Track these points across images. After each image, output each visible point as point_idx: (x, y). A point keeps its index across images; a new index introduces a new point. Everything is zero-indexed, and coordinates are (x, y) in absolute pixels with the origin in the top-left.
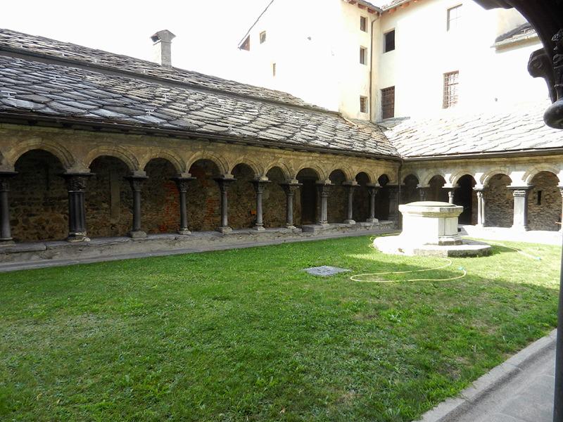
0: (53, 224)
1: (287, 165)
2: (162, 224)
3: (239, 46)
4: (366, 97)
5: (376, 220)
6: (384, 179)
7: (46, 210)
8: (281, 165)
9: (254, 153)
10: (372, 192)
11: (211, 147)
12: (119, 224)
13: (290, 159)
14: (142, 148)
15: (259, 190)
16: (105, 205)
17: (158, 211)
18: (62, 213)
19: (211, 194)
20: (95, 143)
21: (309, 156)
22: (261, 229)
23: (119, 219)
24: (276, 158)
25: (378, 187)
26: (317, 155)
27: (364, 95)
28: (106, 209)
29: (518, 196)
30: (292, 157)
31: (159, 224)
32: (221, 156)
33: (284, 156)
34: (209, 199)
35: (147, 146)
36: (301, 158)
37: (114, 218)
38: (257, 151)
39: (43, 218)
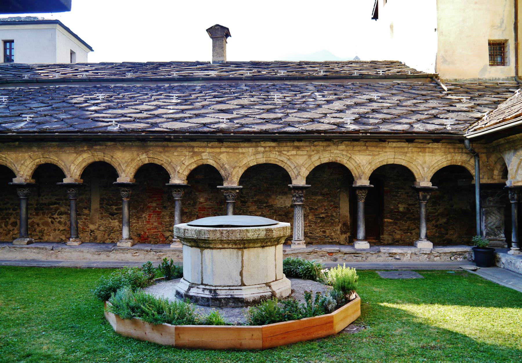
0: (42, 227)
1: (217, 161)
2: (142, 233)
3: (373, 16)
4: (506, 41)
7: (37, 214)
12: (98, 229)
14: (20, 154)
15: (174, 195)
16: (86, 211)
17: (139, 218)
18: (50, 218)
19: (202, 200)
21: (257, 146)
23: (97, 225)
27: (497, 36)
28: (87, 215)
30: (223, 150)
31: (139, 232)
32: (112, 157)
33: (208, 150)
34: (200, 206)
35: (26, 152)
37: (93, 224)
38: (164, 146)
39: (35, 221)
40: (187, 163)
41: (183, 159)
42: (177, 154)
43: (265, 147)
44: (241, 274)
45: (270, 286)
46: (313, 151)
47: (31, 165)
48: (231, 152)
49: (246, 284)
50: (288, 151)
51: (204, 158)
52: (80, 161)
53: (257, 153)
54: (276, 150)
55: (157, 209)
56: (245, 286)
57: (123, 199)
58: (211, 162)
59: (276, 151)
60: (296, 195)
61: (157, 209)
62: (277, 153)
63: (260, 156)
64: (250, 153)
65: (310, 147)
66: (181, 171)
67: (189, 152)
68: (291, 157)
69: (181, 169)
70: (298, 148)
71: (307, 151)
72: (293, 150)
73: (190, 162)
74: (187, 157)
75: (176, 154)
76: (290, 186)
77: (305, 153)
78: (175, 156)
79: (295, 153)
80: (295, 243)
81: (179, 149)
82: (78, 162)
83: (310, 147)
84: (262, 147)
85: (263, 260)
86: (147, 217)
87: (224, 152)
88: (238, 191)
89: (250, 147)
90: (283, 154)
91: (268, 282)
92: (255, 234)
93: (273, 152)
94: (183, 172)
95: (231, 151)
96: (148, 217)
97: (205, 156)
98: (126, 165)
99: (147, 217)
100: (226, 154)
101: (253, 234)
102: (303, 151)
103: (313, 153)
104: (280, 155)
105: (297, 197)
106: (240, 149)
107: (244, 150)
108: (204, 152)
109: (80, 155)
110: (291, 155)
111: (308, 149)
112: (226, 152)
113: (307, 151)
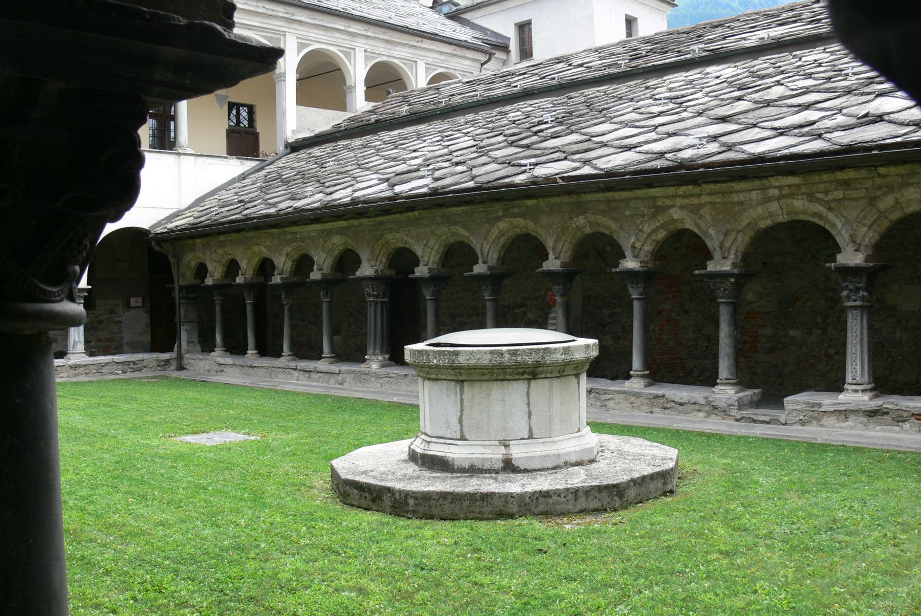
11: (516, 210)
13: (700, 206)
14: (422, 230)
15: (631, 290)
20: (379, 232)
21: (764, 188)
30: (705, 199)
33: (679, 202)
36: (735, 198)
40: (647, 229)
41: (639, 222)
42: (629, 214)
44: (460, 421)
45: (506, 446)
46: (879, 188)
47: (436, 245)
48: (719, 203)
49: (467, 437)
50: (826, 192)
51: (676, 217)
52: (496, 234)
53: (767, 202)
54: (803, 191)
55: (673, 315)
56: (466, 440)
57: (556, 298)
58: (689, 225)
59: (802, 194)
60: (847, 286)
61: (673, 315)
62: (805, 197)
63: (774, 206)
64: (754, 202)
65: (872, 178)
66: (638, 245)
67: (649, 207)
68: (832, 205)
69: (638, 240)
70: (847, 184)
71: (866, 189)
72: (835, 190)
73: (653, 227)
74: (646, 218)
75: (628, 213)
76: (830, 268)
77: (862, 193)
78: (627, 216)
79: (841, 196)
81: (632, 204)
82: (493, 237)
83: (872, 178)
84: (776, 187)
85: (496, 402)
86: (657, 329)
87: (706, 204)
88: (733, 280)
89: (752, 190)
90: (818, 199)
91: (508, 438)
92: (472, 358)
93: (796, 197)
94: (643, 245)
95: (718, 200)
96: (659, 330)
97: (676, 214)
98: (554, 238)
99: (657, 329)
100: (709, 206)
101: (468, 357)
102: (857, 189)
103: (879, 193)
104: (811, 201)
105: (851, 291)
106: (734, 195)
107: (742, 197)
108: (673, 206)
109: (494, 225)
110: (834, 200)
111: (869, 184)
112: (711, 203)
113: (866, 189)
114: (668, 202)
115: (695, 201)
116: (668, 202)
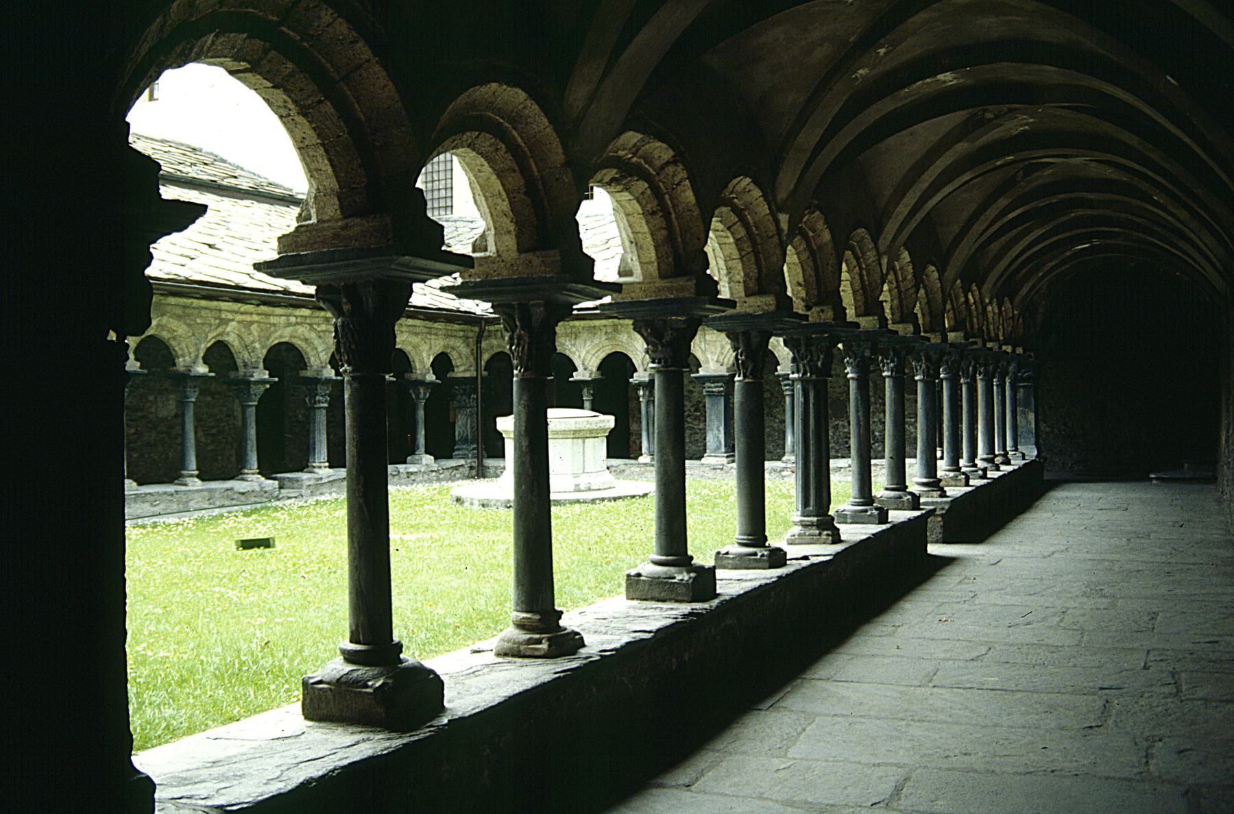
5: (428, 459)
6: (442, 363)
8: (232, 340)
9: (179, 311)
10: (418, 394)
21: (288, 316)
22: (196, 484)
24: (226, 322)
25: (431, 383)
26: (306, 312)
29: (711, 394)
30: (255, 318)
33: (239, 317)
36: (273, 320)
43: (296, 317)
50: (319, 325)
78: (198, 324)
80: (320, 467)
81: (203, 313)
106: (271, 317)
108: (233, 320)
110: (322, 331)
114: (230, 316)
115: (248, 318)
116: (230, 316)
